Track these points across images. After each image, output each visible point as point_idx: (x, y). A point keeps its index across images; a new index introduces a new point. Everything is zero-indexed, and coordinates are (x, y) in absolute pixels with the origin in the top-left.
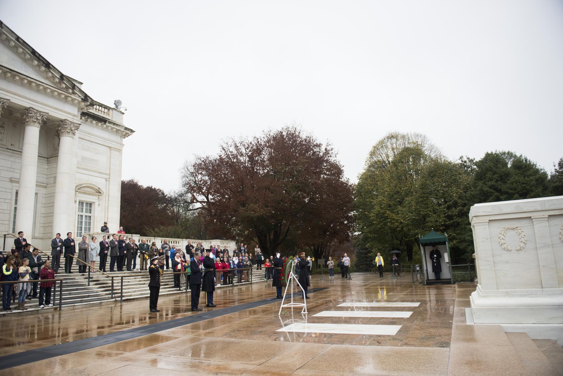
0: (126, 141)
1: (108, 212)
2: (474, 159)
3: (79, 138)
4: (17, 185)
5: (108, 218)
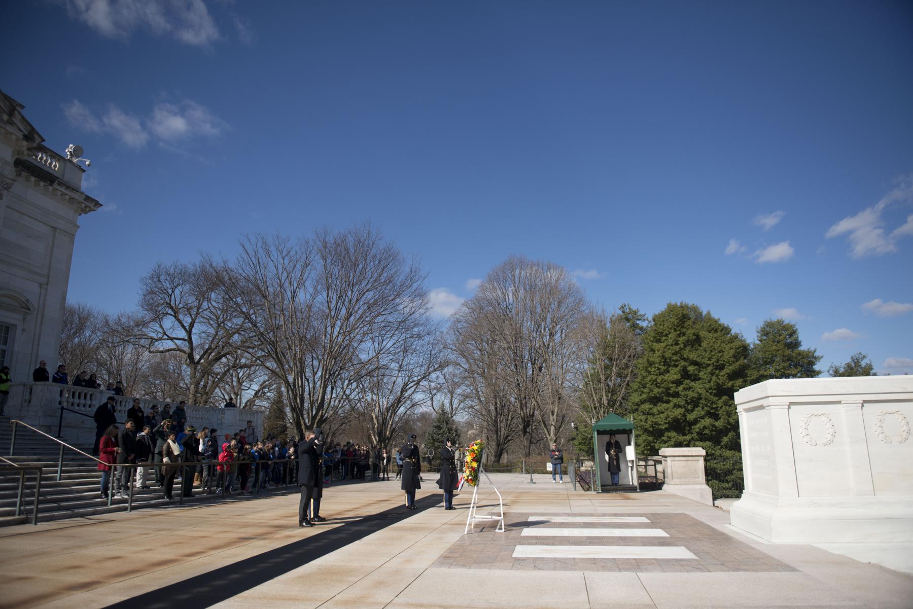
0: (82, 220)
1: (38, 345)
2: (639, 311)
3: (7, 206)
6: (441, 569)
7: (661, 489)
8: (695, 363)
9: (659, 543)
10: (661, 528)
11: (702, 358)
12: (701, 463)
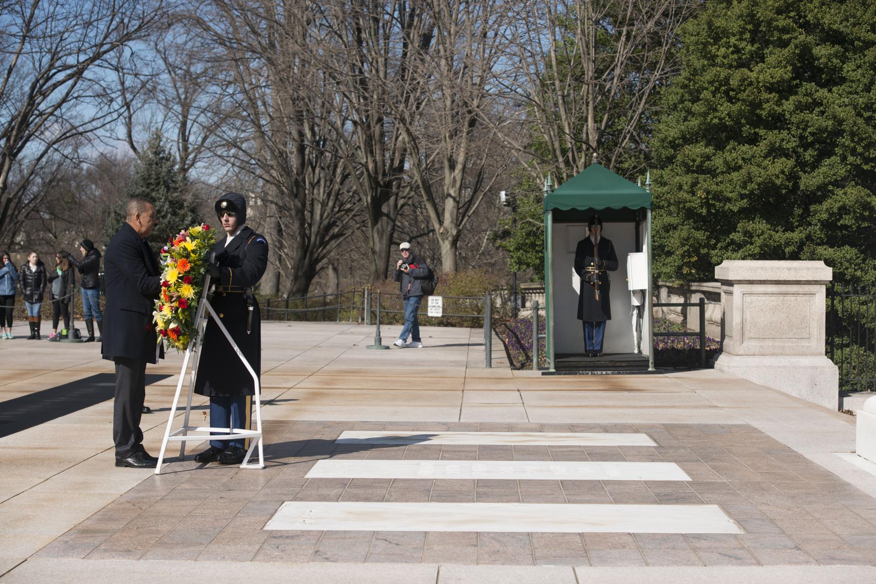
6: (64, 560)
7: (712, 367)
8: (833, 37)
9: (657, 495)
10: (675, 461)
11: (854, 25)
12: (819, 301)
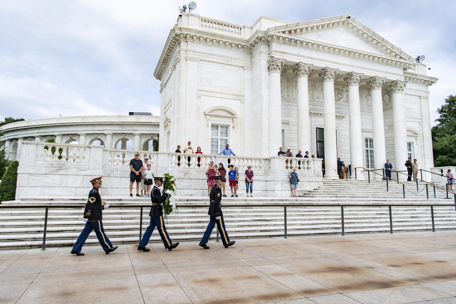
3: (405, 94)
4: (371, 134)
5: (424, 154)
